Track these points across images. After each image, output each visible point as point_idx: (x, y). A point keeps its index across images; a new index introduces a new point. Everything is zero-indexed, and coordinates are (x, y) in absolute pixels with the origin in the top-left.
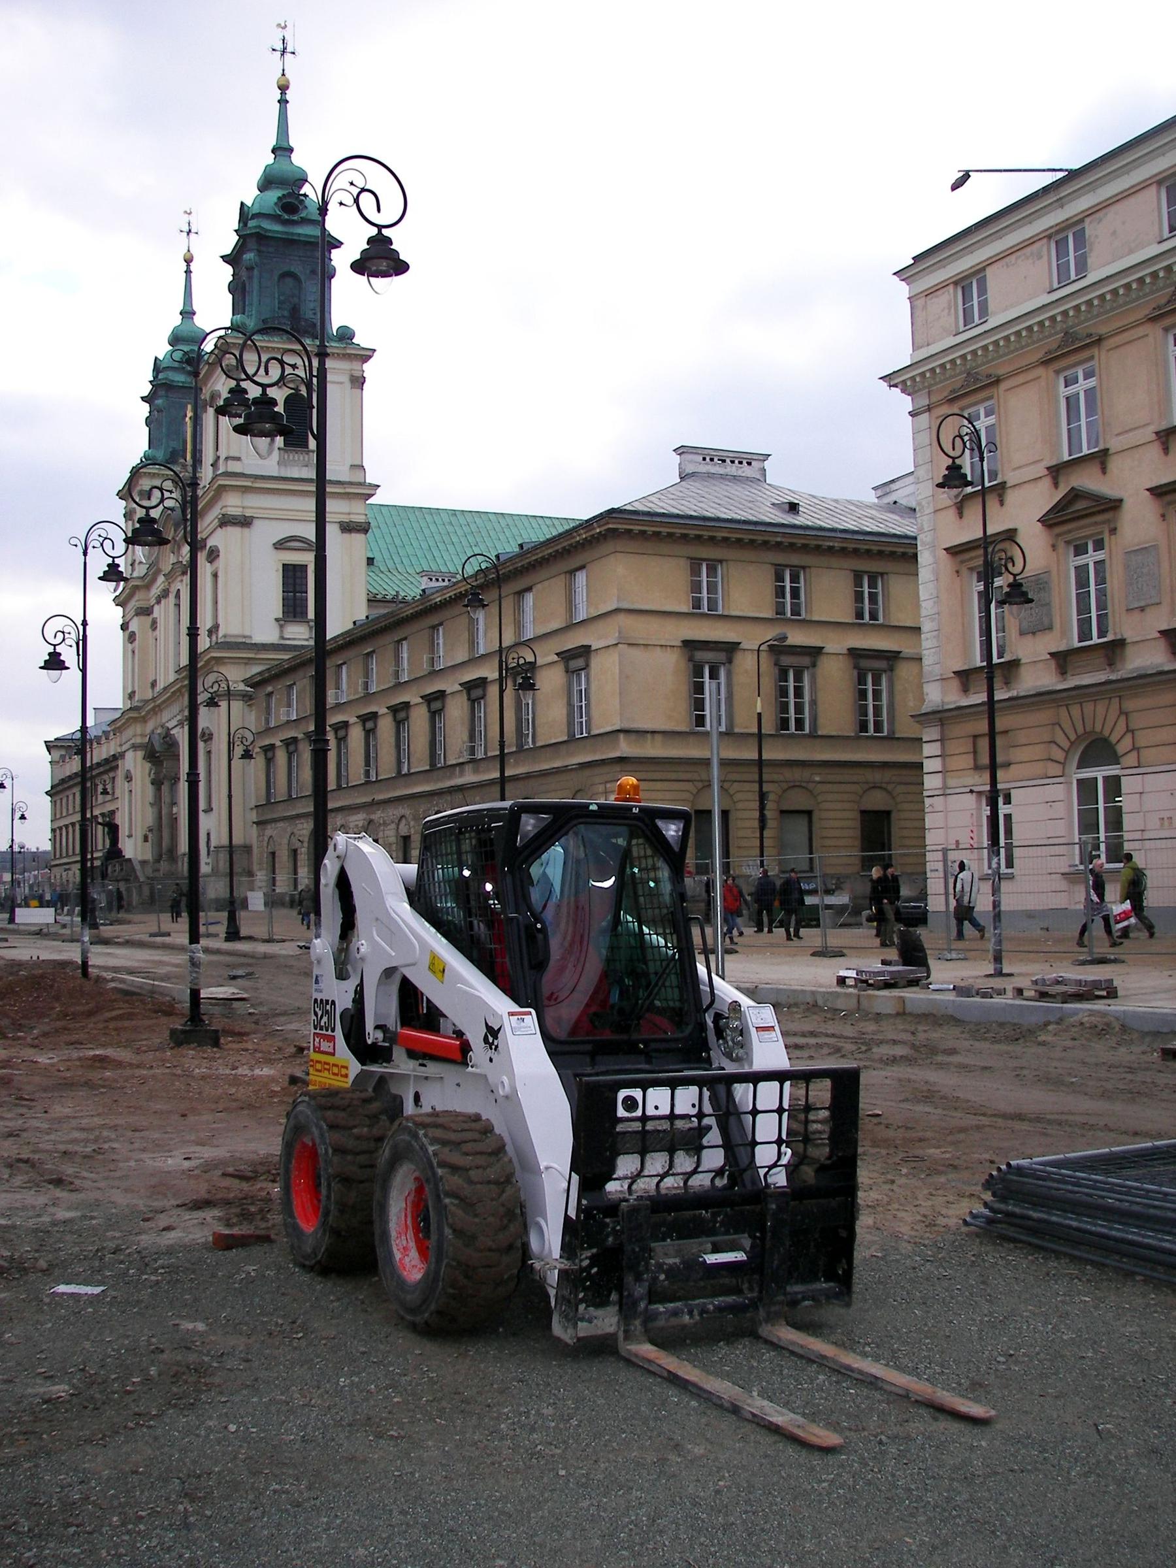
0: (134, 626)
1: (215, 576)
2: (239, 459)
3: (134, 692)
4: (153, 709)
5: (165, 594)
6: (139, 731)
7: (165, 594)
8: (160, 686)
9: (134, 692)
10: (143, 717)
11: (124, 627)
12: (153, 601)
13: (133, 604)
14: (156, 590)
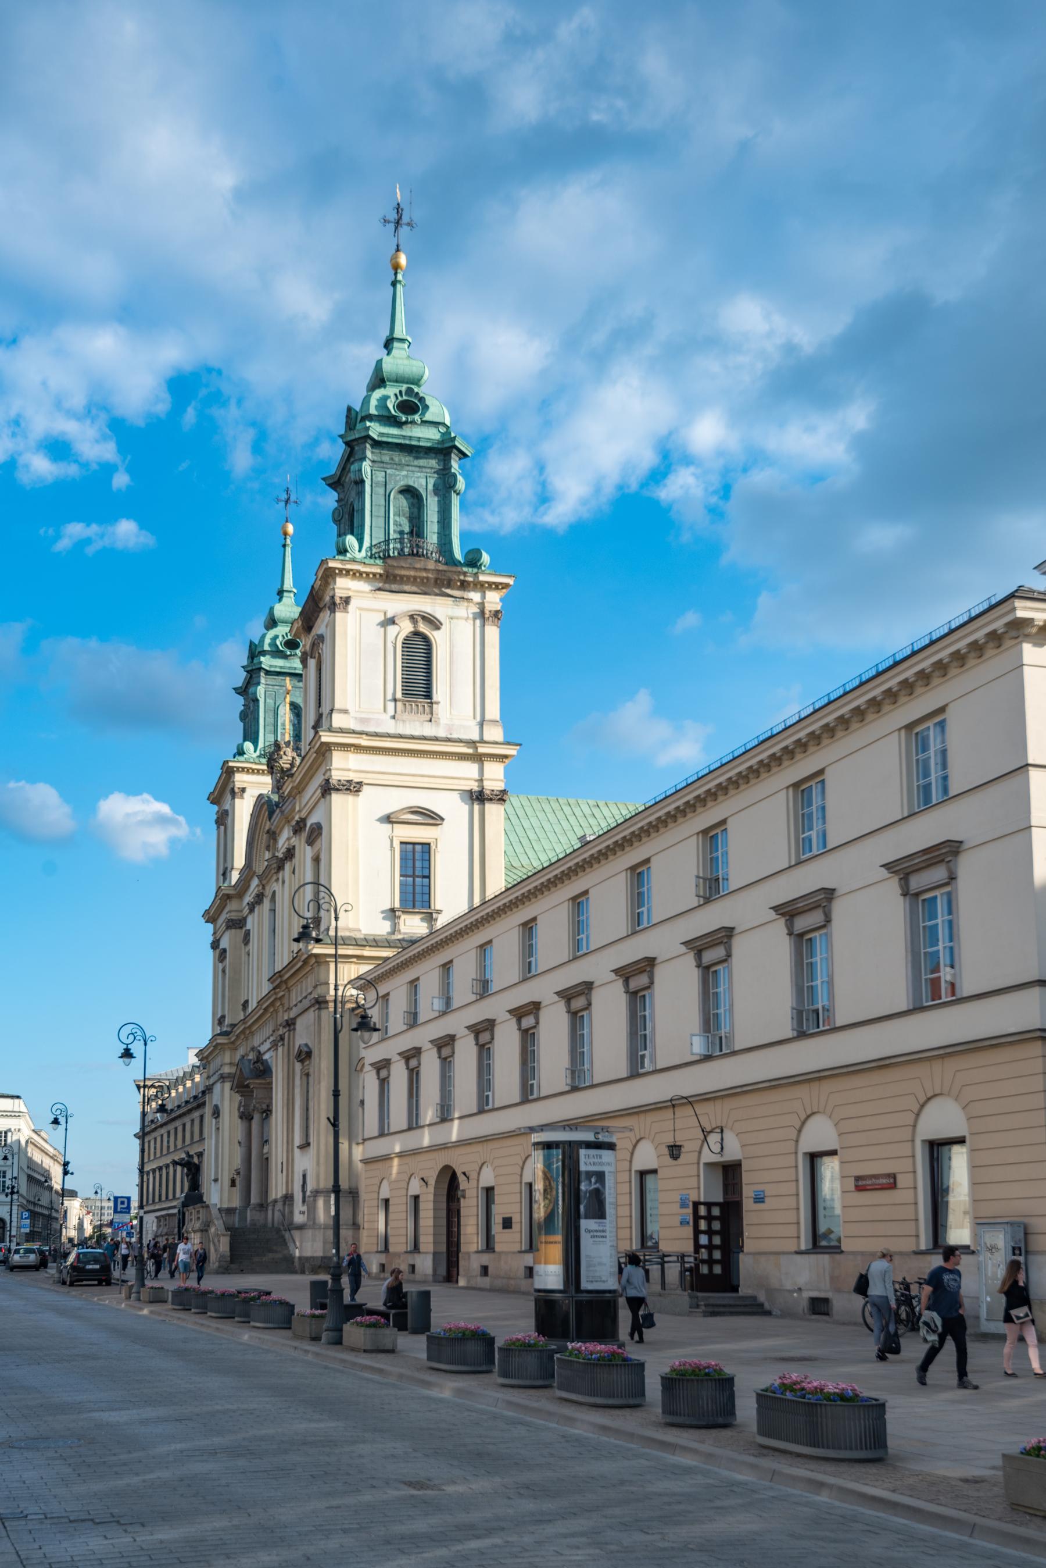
0: (224, 943)
1: (317, 860)
2: (346, 712)
3: (223, 1017)
4: (243, 1032)
5: (259, 898)
6: (227, 1060)
7: (259, 898)
8: (253, 1005)
9: (223, 1017)
10: (233, 1043)
11: (215, 945)
12: (246, 911)
13: (221, 920)
14: (248, 898)
